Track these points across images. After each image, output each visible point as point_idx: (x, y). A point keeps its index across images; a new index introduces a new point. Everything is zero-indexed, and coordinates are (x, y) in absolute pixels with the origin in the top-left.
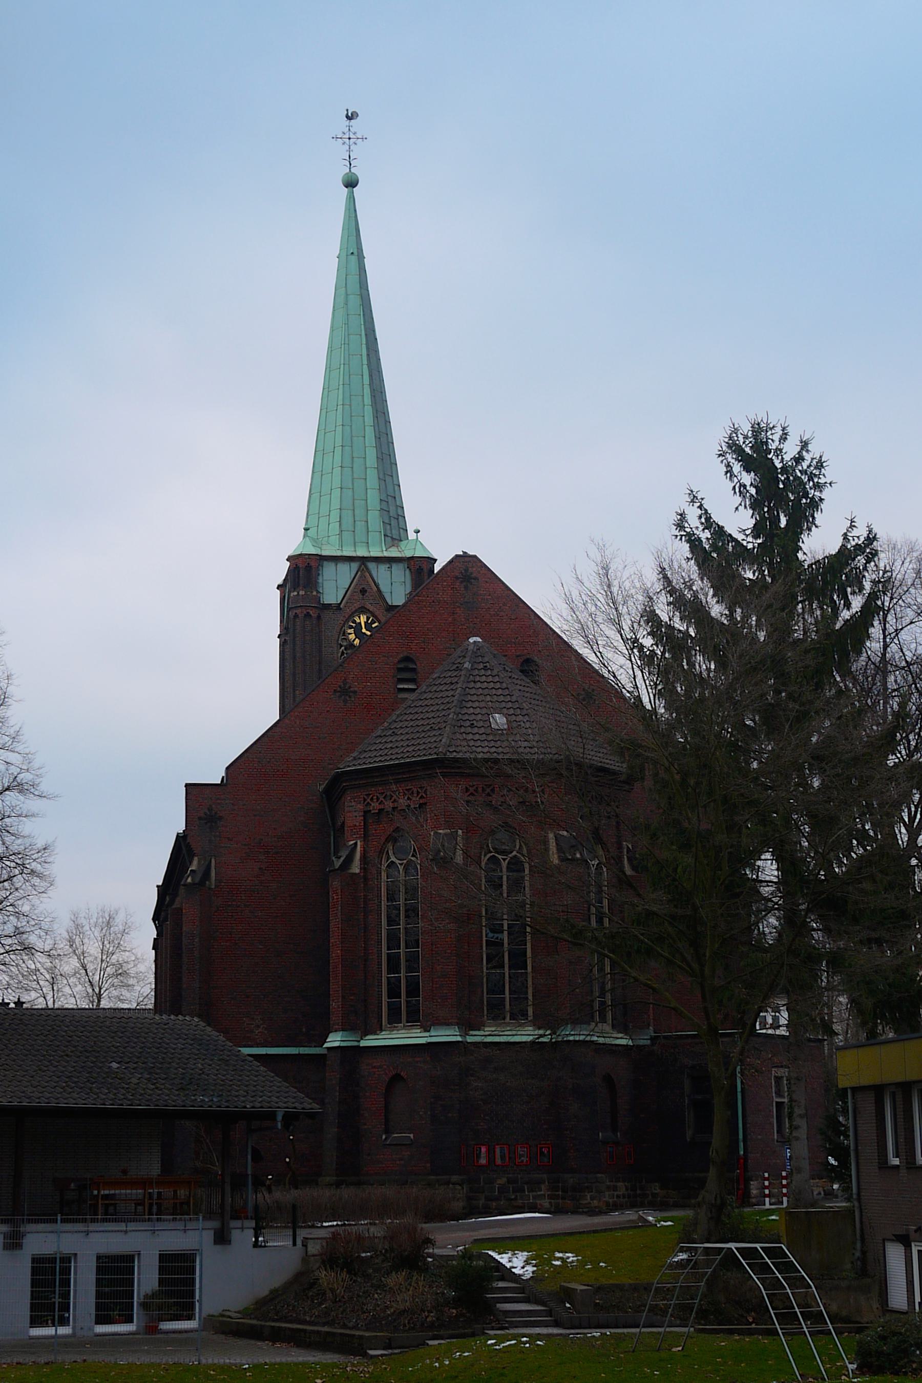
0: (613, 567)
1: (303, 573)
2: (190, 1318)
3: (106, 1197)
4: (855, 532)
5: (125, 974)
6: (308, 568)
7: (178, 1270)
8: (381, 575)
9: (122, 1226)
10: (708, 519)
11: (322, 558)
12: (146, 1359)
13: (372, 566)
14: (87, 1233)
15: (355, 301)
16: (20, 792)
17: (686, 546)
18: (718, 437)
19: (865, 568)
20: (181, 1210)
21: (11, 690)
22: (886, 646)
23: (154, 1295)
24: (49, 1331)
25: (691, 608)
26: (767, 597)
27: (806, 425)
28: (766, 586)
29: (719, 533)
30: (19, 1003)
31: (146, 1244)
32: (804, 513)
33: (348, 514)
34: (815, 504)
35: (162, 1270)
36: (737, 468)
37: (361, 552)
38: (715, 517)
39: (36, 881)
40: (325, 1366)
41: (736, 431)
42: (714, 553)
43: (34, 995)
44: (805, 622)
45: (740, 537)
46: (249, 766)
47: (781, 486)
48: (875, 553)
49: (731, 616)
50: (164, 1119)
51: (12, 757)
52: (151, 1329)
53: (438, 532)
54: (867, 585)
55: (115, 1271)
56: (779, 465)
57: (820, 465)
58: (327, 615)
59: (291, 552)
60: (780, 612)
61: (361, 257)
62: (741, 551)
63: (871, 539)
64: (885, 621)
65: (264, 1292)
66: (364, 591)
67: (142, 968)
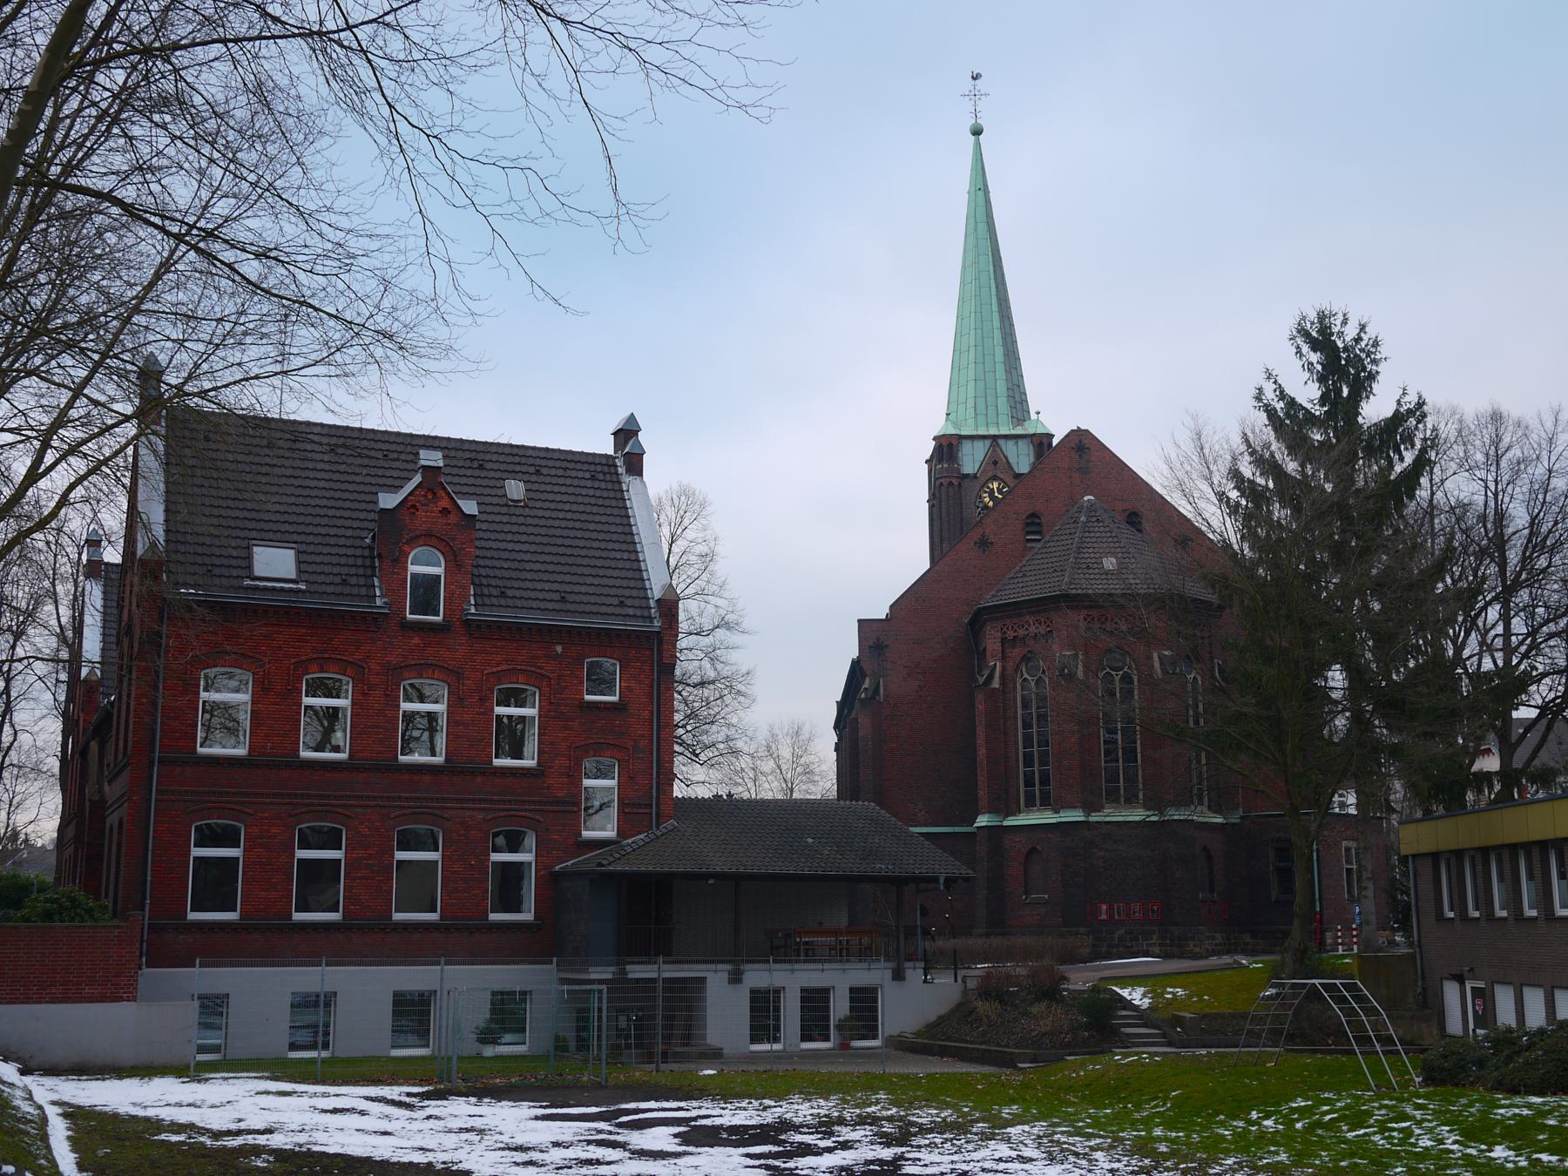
0: (1204, 433)
1: (946, 450)
2: (875, 1037)
3: (806, 943)
4: (1407, 399)
5: (811, 772)
6: (950, 446)
7: (864, 1001)
8: (1009, 449)
9: (820, 966)
10: (1282, 392)
11: (961, 438)
12: (842, 1069)
13: (1001, 442)
14: (792, 971)
15: (982, 227)
16: (729, 629)
17: (1265, 415)
18: (1289, 324)
19: (1416, 428)
20: (865, 954)
21: (718, 549)
22: (1433, 494)
23: (846, 1020)
24: (766, 1047)
25: (1267, 465)
26: (1334, 454)
27: (1361, 310)
28: (1332, 447)
29: (1292, 403)
30: (730, 795)
31: (842, 981)
32: (1362, 384)
33: (981, 402)
34: (1372, 377)
35: (852, 1000)
36: (1305, 349)
37: (993, 431)
38: (1288, 391)
39: (741, 699)
40: (984, 1076)
41: (1304, 318)
42: (1288, 420)
43: (741, 789)
44: (1365, 472)
45: (1309, 406)
46: (911, 603)
47: (1342, 364)
48: (1424, 415)
49: (1303, 473)
50: (851, 880)
51: (720, 602)
52: (844, 1046)
53: (1055, 417)
54: (1418, 445)
55: (814, 1002)
56: (1340, 345)
57: (1376, 344)
58: (966, 483)
59: (936, 433)
60: (1342, 468)
61: (985, 190)
62: (1310, 418)
63: (1421, 404)
64: (1432, 472)
65: (932, 1018)
66: (996, 463)
67: (824, 767)
